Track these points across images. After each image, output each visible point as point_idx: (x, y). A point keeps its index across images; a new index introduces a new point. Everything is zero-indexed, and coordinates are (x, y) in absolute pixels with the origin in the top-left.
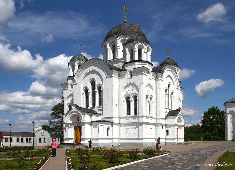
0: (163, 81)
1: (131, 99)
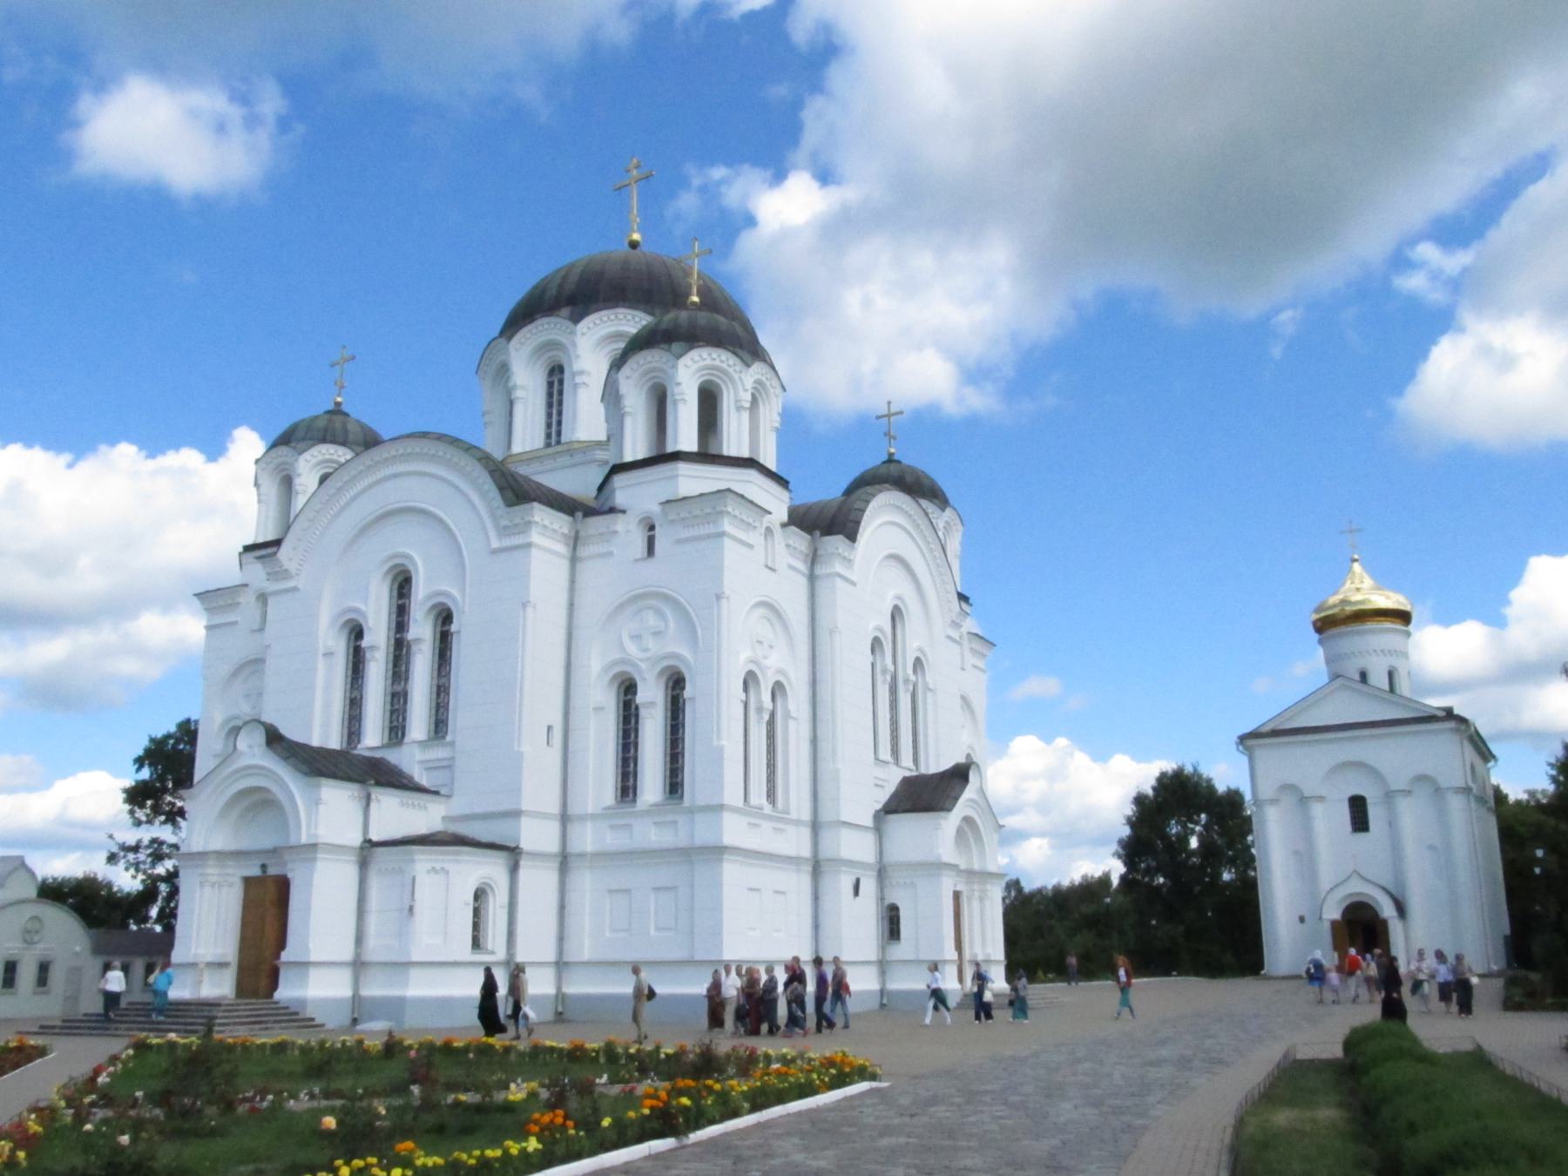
0: (854, 584)
1: (651, 696)
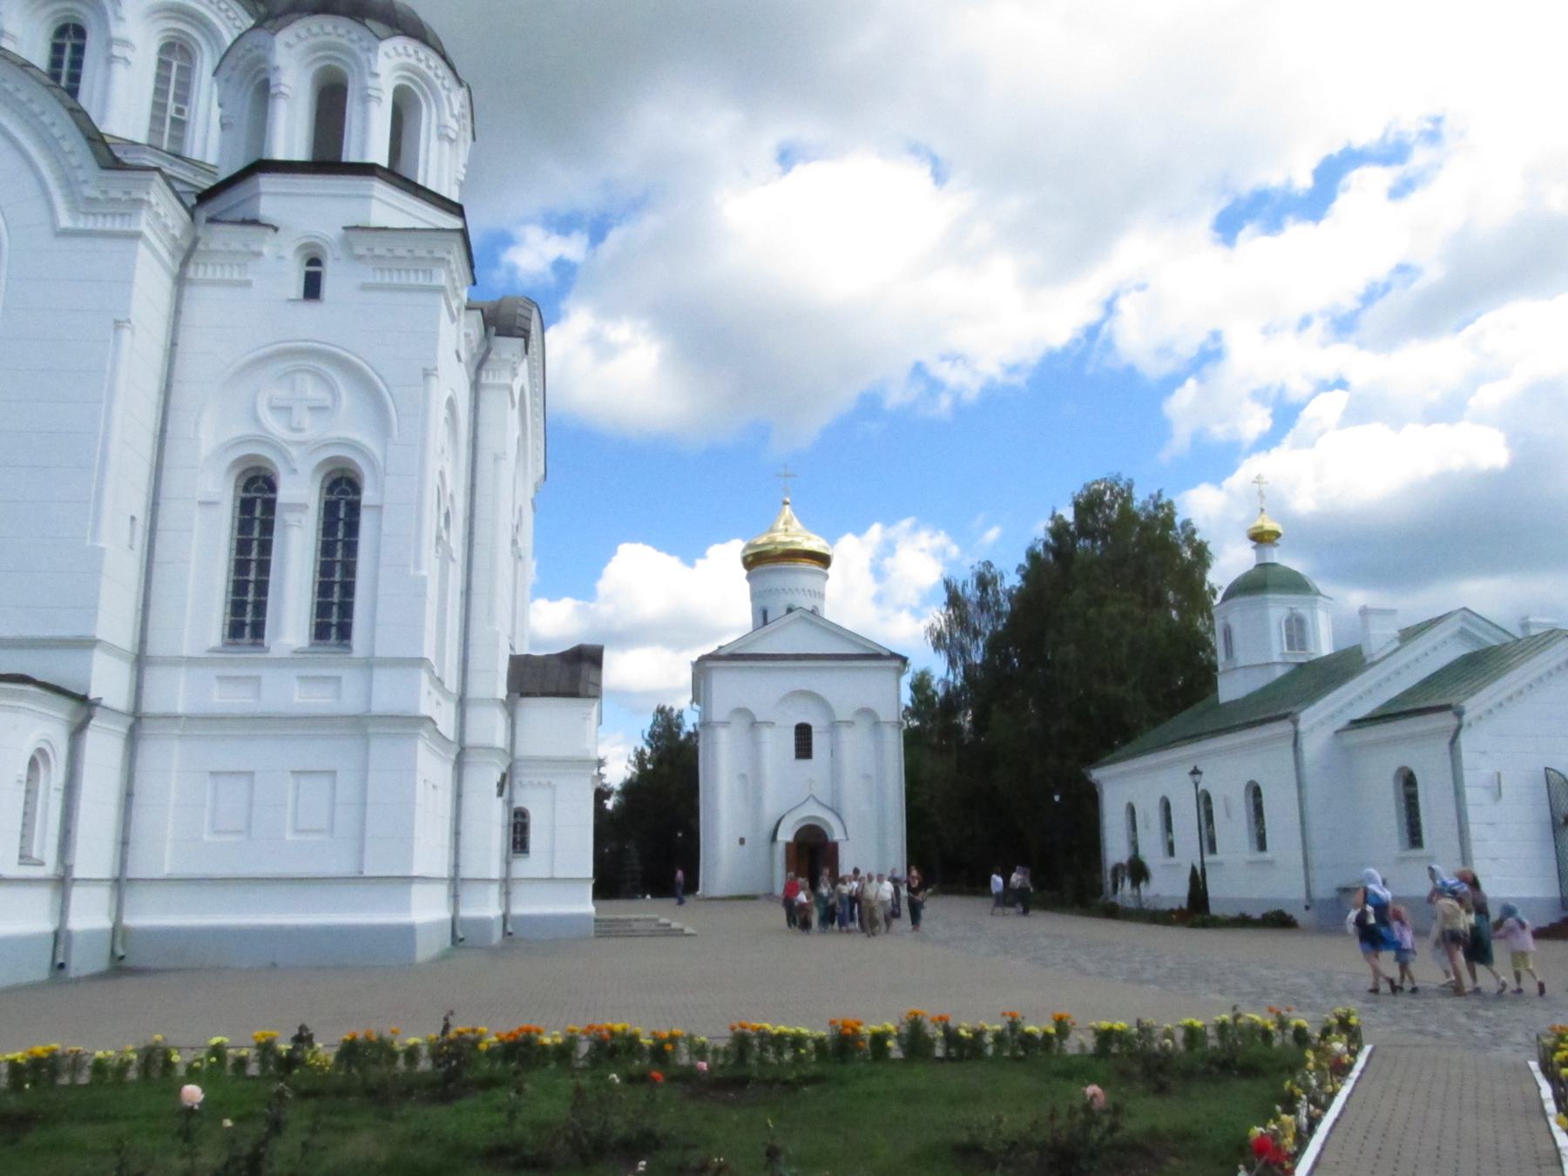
1: (300, 496)
